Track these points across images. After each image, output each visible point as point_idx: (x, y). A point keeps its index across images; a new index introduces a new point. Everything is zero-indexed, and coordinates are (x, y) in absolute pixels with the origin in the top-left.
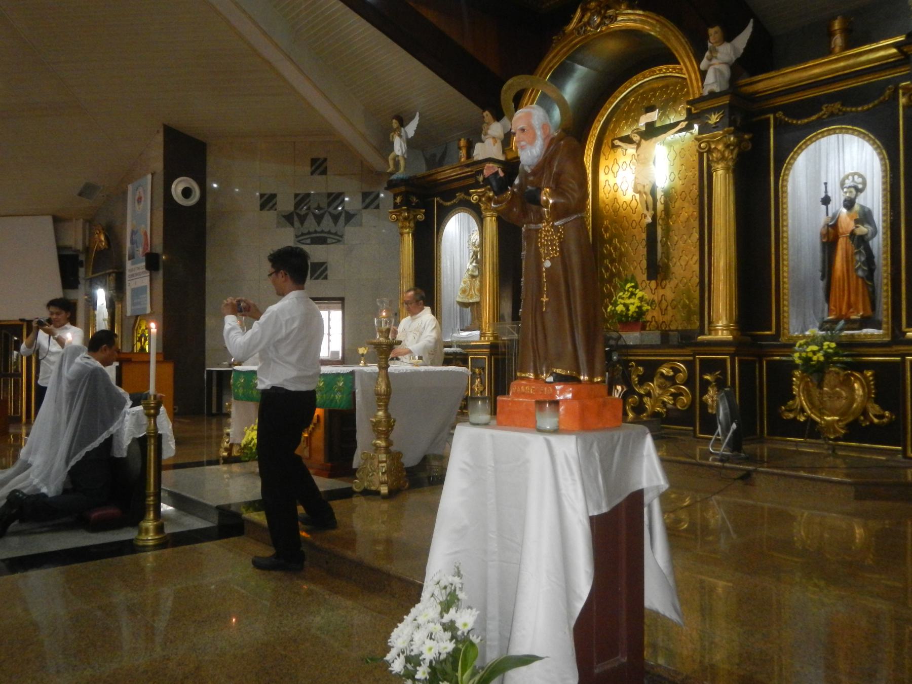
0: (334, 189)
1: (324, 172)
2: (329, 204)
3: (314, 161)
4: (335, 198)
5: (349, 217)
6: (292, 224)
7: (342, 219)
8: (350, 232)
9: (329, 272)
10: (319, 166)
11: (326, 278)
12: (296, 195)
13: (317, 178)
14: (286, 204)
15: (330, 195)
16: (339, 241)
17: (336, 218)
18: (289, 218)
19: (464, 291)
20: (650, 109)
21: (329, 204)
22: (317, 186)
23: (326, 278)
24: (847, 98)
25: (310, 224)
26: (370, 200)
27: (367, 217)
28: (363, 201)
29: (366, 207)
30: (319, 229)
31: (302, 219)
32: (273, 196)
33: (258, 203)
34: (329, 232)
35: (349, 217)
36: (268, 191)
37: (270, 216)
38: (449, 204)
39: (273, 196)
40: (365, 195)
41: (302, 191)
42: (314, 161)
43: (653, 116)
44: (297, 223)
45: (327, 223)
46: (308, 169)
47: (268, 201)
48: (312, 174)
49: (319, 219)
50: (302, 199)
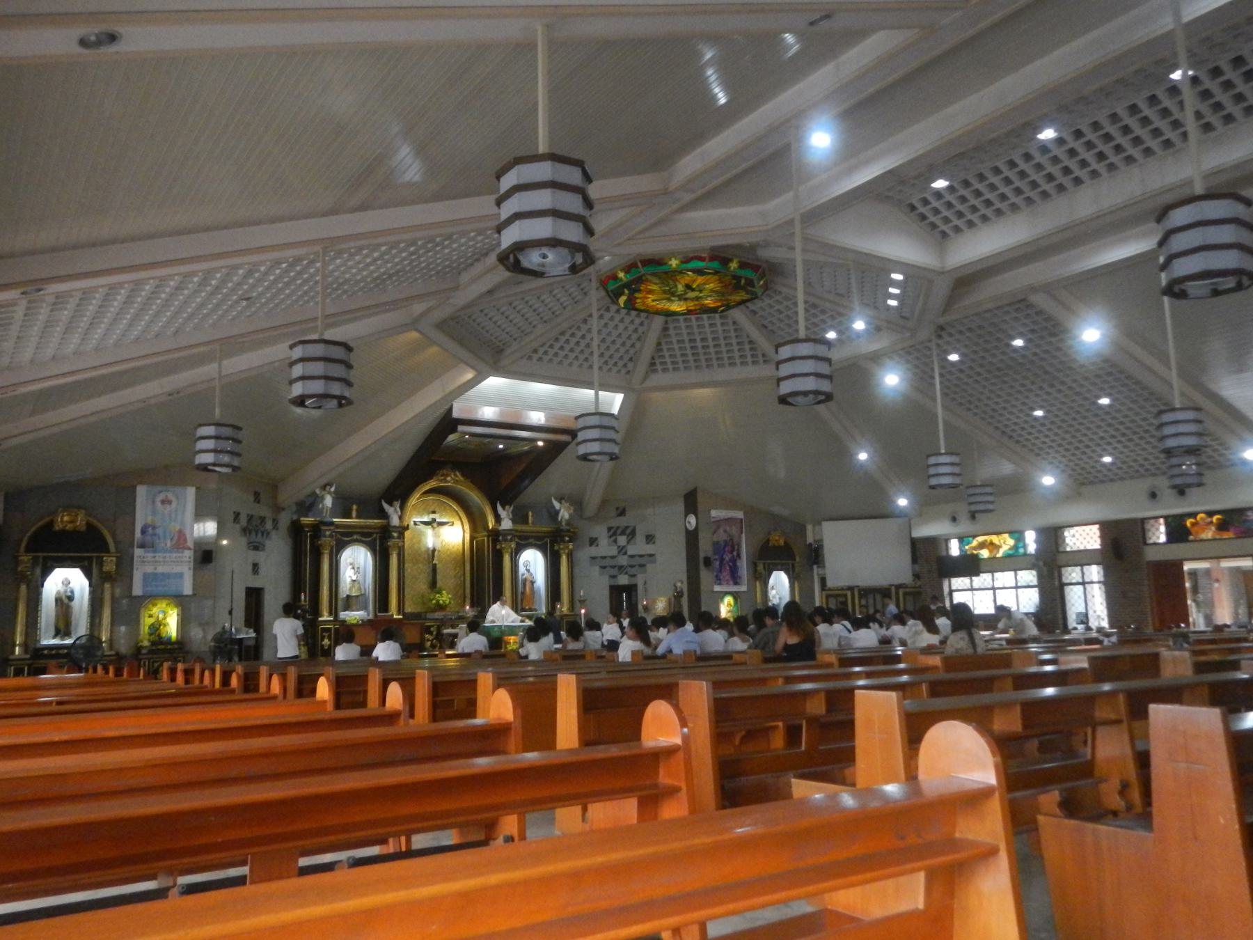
0: (262, 514)
1: (259, 502)
6: (245, 534)
8: (268, 543)
12: (248, 515)
14: (243, 520)
19: (350, 589)
20: (434, 512)
24: (538, 538)
30: (256, 540)
33: (232, 518)
34: (260, 543)
37: (238, 527)
38: (346, 539)
41: (250, 513)
43: (437, 517)
46: (252, 498)
47: (237, 516)
49: (257, 532)
50: (250, 518)
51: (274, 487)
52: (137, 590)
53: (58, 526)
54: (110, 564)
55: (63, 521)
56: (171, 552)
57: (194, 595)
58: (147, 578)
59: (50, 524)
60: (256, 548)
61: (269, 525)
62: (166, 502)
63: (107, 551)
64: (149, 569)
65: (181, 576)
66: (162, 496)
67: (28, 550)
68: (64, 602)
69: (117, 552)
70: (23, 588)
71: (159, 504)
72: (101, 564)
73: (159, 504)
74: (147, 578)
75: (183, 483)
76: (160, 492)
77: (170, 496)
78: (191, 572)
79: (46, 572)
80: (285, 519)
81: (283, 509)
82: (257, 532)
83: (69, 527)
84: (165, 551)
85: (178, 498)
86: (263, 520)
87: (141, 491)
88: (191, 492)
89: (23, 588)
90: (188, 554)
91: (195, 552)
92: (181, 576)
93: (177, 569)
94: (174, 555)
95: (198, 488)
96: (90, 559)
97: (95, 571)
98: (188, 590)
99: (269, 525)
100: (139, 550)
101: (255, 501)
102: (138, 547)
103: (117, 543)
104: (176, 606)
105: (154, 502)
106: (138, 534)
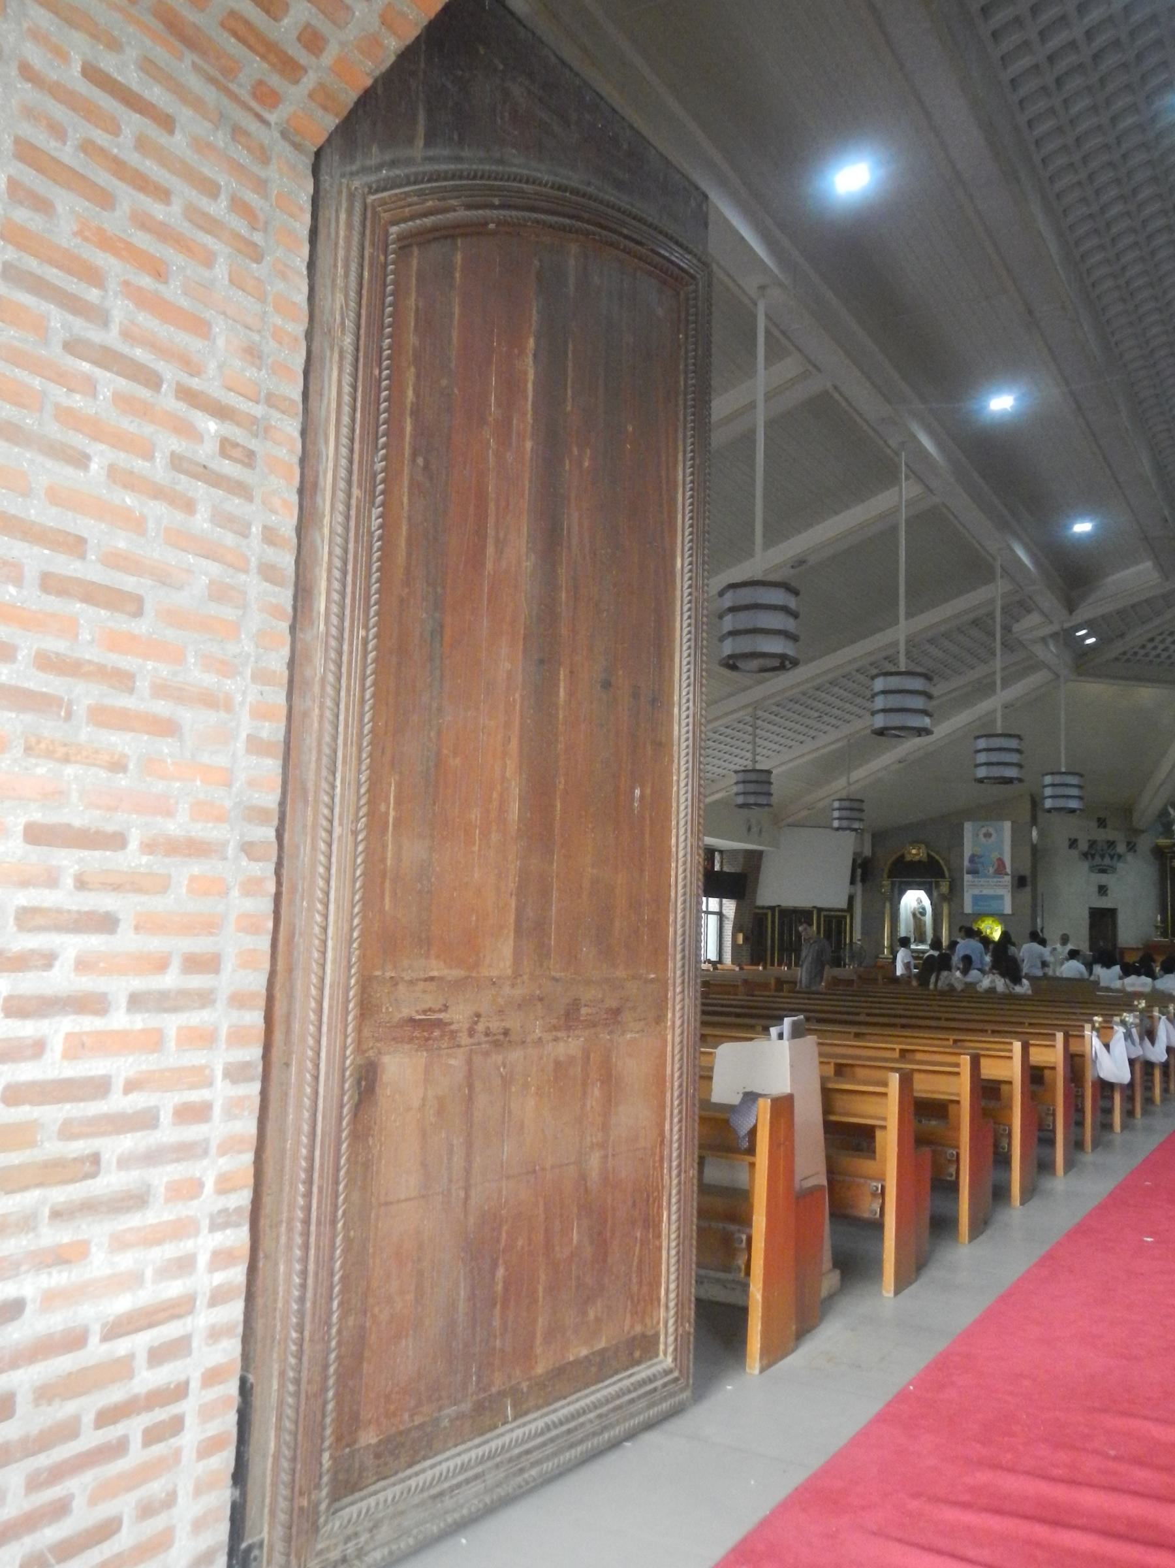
0: (1111, 838)
1: (1105, 827)
2: (1109, 847)
3: (1099, 819)
4: (1111, 844)
5: (1120, 856)
7: (1116, 857)
8: (1120, 865)
9: (1109, 892)
10: (1102, 823)
11: (1107, 895)
13: (1102, 830)
14: (1083, 846)
15: (1108, 842)
16: (1113, 872)
17: (1112, 857)
18: (1085, 855)
21: (1109, 847)
22: (1101, 835)
23: (1107, 895)
25: (1098, 860)
26: (1131, 847)
27: (1130, 857)
28: (1127, 846)
29: (1129, 850)
31: (1093, 856)
32: (1076, 841)
33: (1067, 843)
35: (1120, 856)
36: (1073, 837)
37: (1075, 853)
39: (1076, 841)
40: (1128, 843)
42: (1099, 819)
44: (1090, 857)
45: (1107, 861)
46: (1094, 824)
47: (1073, 843)
48: (1099, 827)
49: (1103, 857)
50: (1092, 844)
51: (1126, 811)
52: (968, 908)
53: (908, 858)
54: (944, 888)
55: (915, 853)
56: (994, 877)
57: (1013, 914)
58: (976, 899)
59: (903, 856)
60: (1103, 871)
61: (1121, 848)
62: (988, 835)
63: (943, 876)
64: (976, 892)
65: (1001, 897)
66: (984, 830)
67: (889, 877)
68: (918, 915)
69: (950, 877)
70: (888, 905)
71: (981, 836)
72: (938, 885)
73: (981, 836)
74: (976, 899)
75: (1001, 817)
76: (983, 827)
77: (991, 830)
78: (1010, 894)
79: (902, 893)
80: (1145, 843)
81: (1143, 832)
82: (1103, 857)
83: (917, 858)
84: (986, 876)
85: (997, 831)
86: (1111, 844)
87: (968, 827)
88: (1007, 825)
89: (888, 905)
90: (1008, 879)
91: (1013, 877)
92: (1001, 898)
93: (1000, 892)
94: (995, 880)
95: (1013, 822)
96: (931, 882)
97: (935, 894)
98: (1008, 910)
99: (1121, 848)
100: (970, 876)
101: (1099, 827)
102: (968, 873)
103: (949, 870)
104: (1001, 924)
105: (978, 835)
106: (966, 863)
